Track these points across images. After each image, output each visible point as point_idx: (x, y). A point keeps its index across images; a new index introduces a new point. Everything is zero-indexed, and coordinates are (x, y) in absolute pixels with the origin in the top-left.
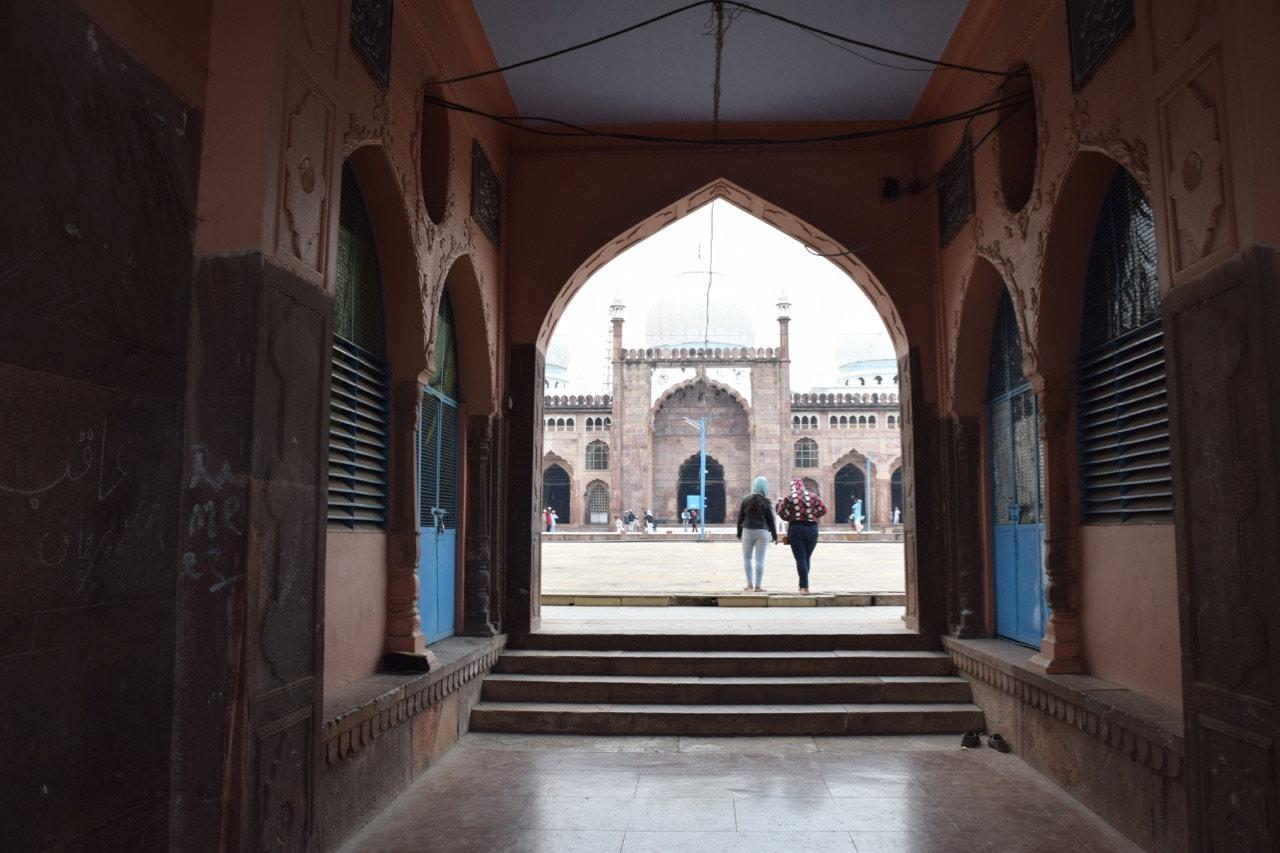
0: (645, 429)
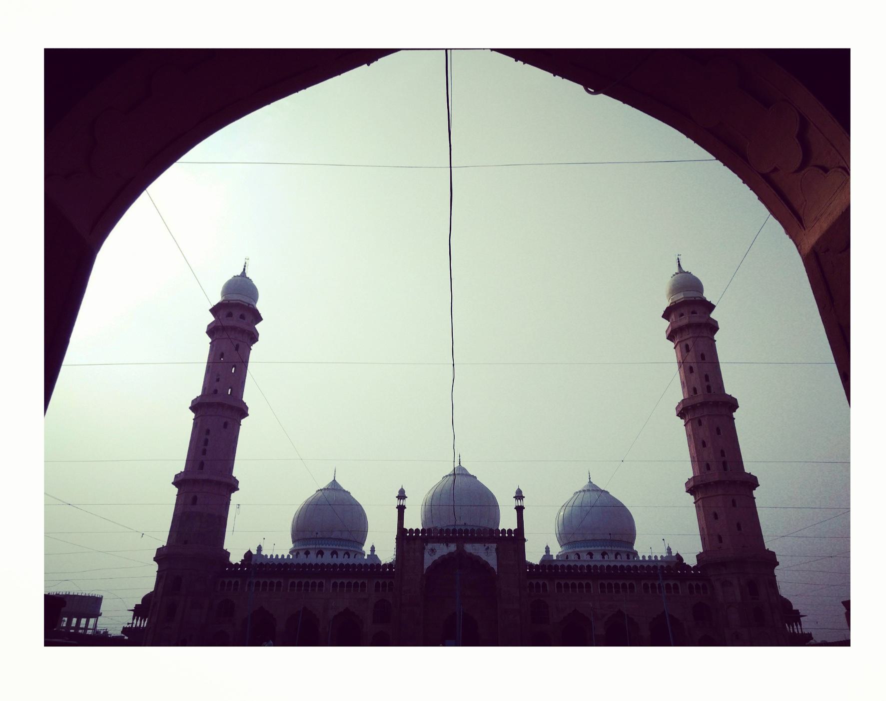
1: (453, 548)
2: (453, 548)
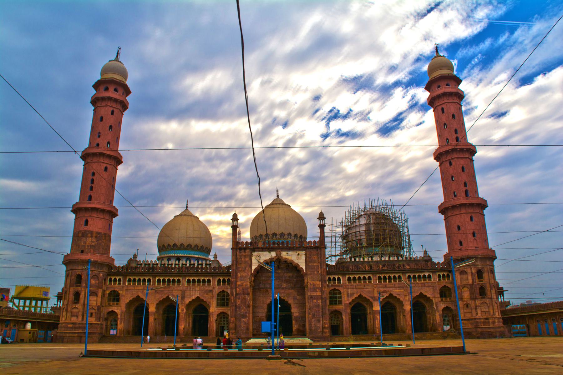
1: (273, 254)
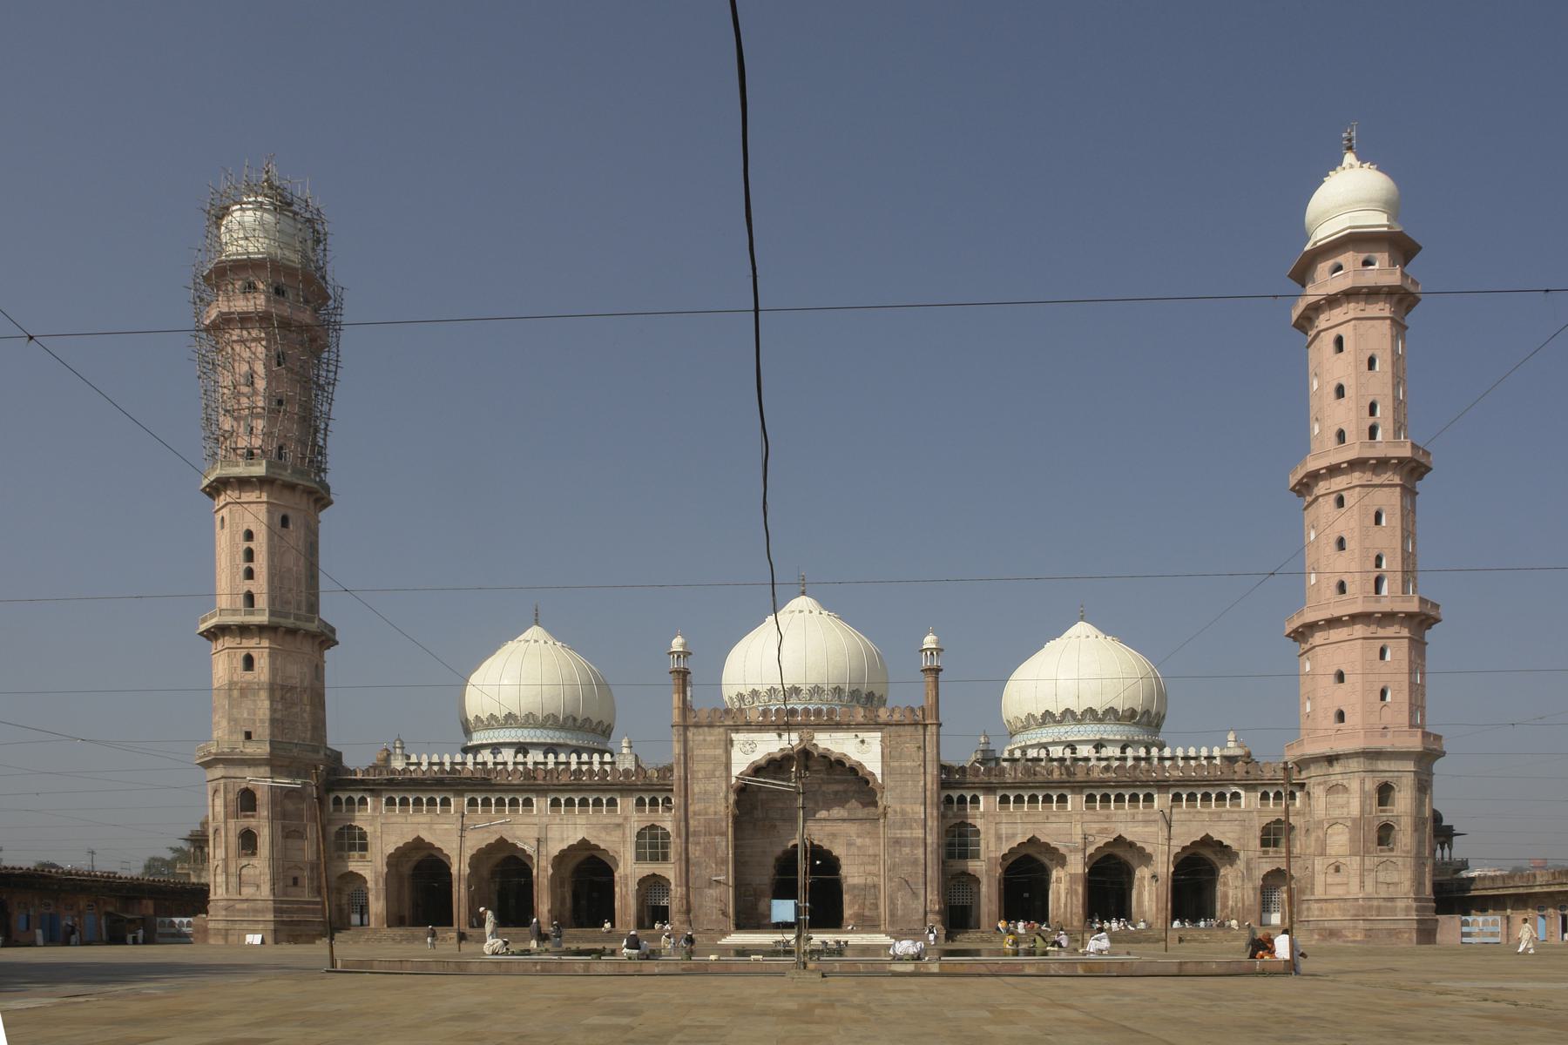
0: (722, 809)
2: (792, 740)
